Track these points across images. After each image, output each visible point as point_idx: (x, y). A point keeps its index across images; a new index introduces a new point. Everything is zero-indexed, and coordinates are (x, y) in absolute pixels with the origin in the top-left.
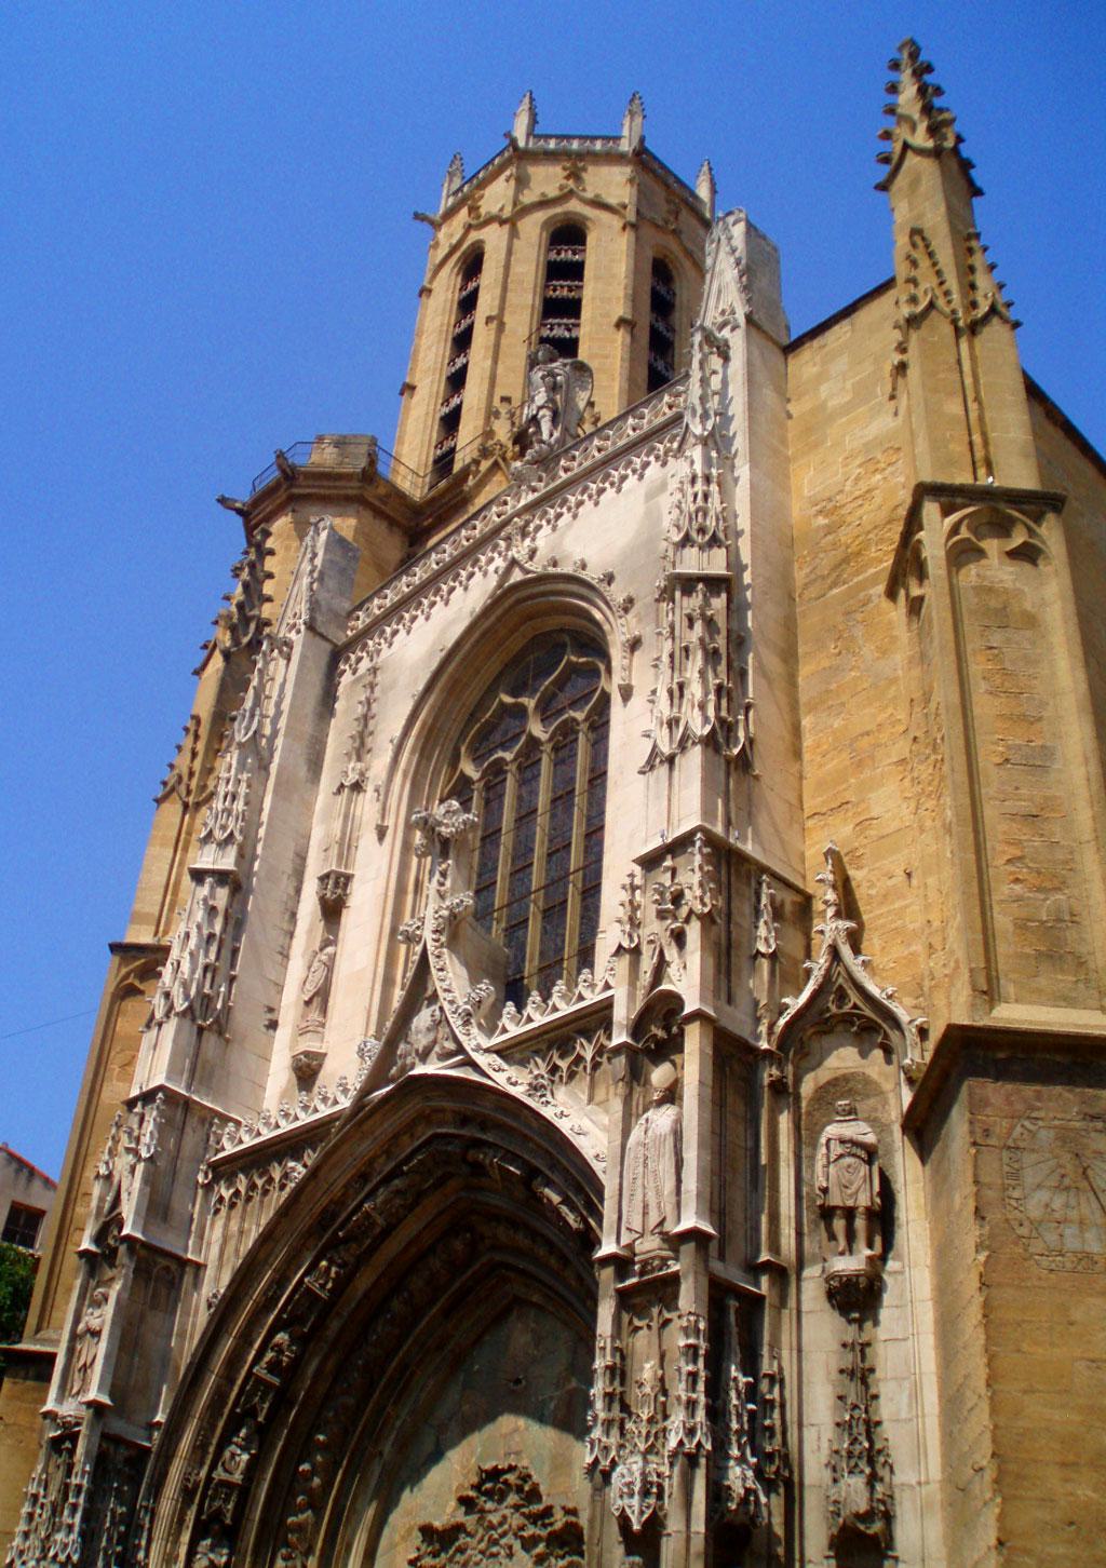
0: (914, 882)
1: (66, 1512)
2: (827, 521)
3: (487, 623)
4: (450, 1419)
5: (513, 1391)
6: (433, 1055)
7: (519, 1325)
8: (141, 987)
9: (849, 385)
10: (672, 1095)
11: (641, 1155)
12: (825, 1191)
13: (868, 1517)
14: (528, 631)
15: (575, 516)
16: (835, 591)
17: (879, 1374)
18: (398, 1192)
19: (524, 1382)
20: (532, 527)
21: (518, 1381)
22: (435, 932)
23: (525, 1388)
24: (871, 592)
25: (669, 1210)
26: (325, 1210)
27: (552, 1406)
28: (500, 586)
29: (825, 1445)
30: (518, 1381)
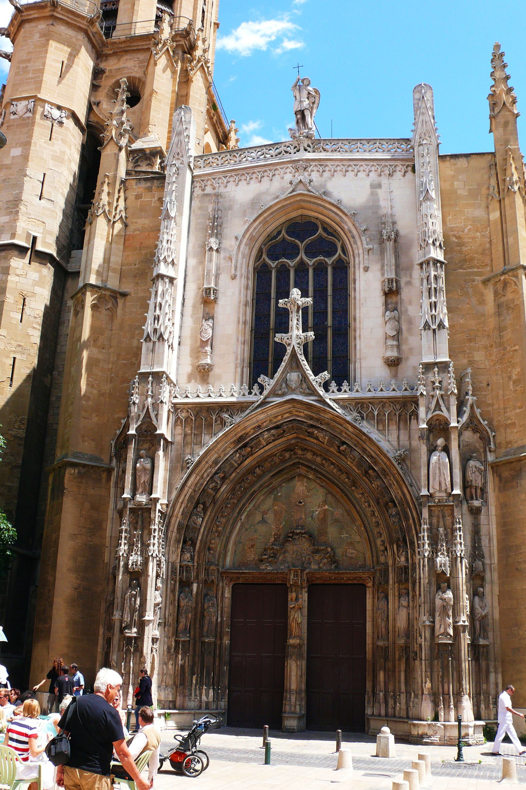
0: (490, 388)
1: (152, 539)
2: (457, 241)
3: (285, 204)
4: (268, 510)
5: (299, 506)
6: (297, 390)
7: (299, 483)
8: (99, 306)
9: (467, 188)
10: (446, 449)
11: (437, 465)
12: (471, 481)
13: (481, 572)
14: (300, 212)
15: (333, 176)
16: (460, 270)
17: (481, 533)
18: (274, 435)
19: (303, 503)
20: (309, 169)
21: (300, 502)
22: (299, 344)
23: (304, 505)
24: (476, 278)
25: (449, 486)
26: (241, 436)
27: (317, 513)
28: (293, 191)
29: (469, 551)
30: (300, 502)
